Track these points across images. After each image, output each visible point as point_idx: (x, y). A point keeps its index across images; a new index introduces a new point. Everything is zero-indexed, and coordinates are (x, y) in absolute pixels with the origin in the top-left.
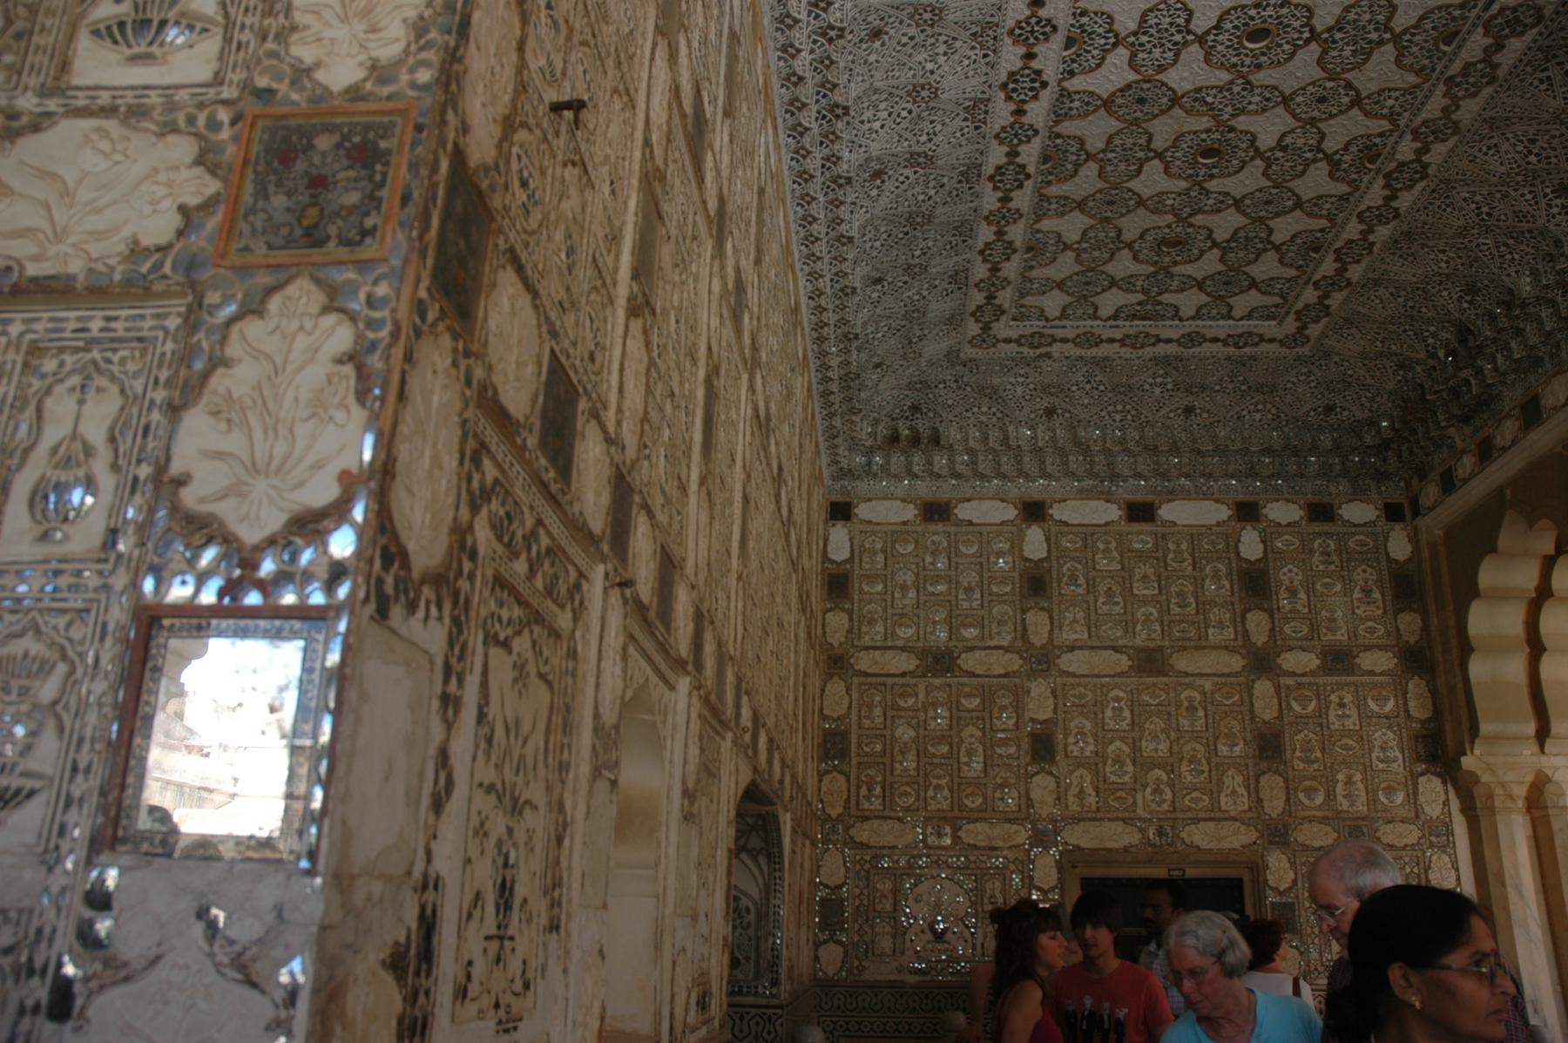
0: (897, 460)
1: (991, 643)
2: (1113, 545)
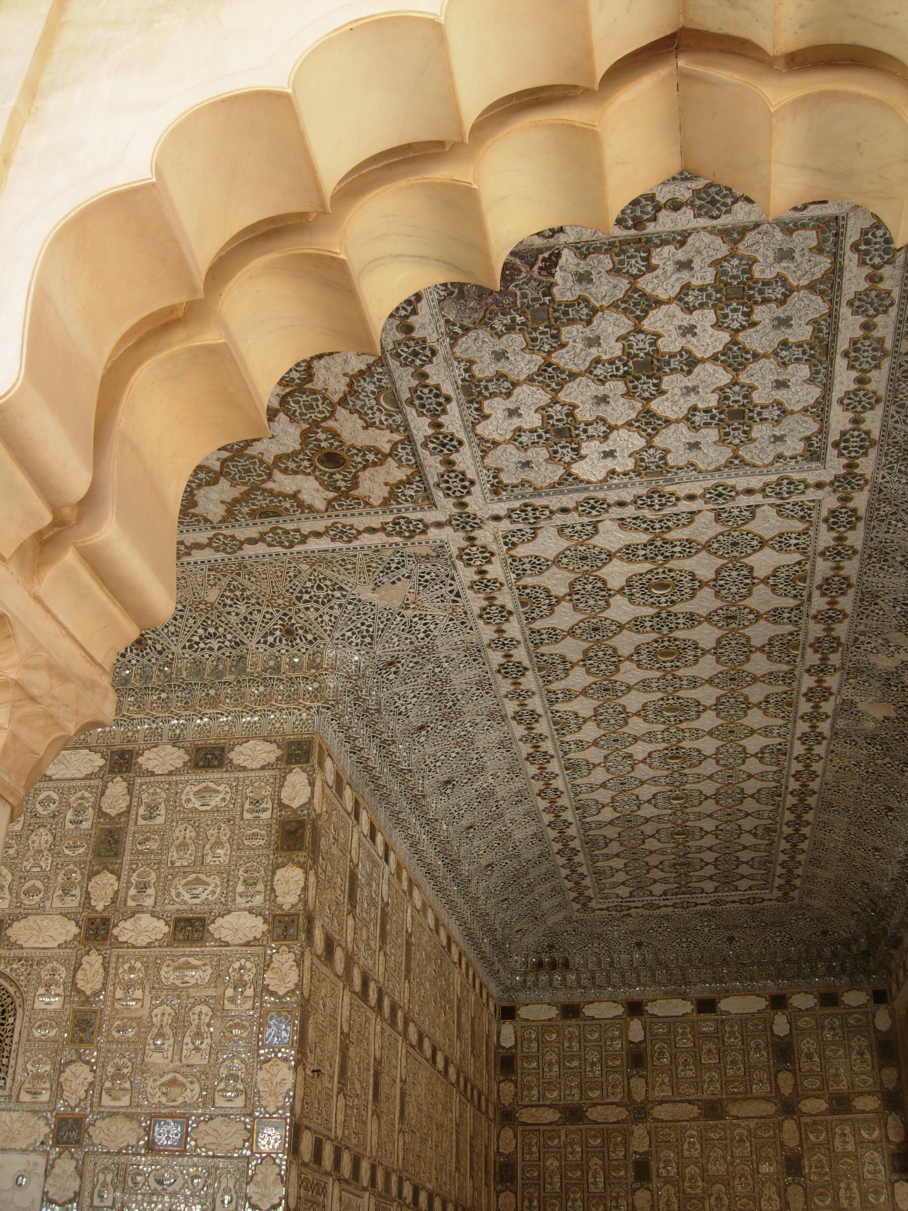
0: (544, 978)
1: (608, 1101)
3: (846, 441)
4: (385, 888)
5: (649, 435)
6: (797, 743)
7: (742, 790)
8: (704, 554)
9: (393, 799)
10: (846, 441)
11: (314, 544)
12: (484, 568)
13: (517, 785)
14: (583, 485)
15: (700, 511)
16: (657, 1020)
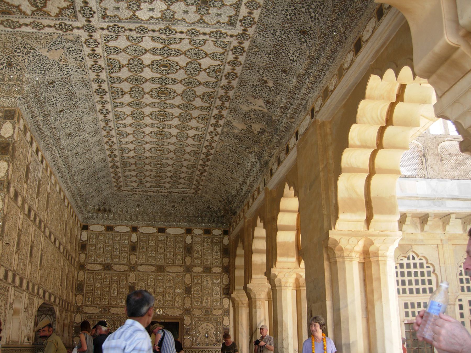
0: (100, 215)
1: (121, 263)
2: (154, 239)
3: (245, 20)
4: (41, 174)
5: (169, 4)
6: (208, 135)
7: (185, 150)
8: (183, 56)
9: (47, 139)
10: (245, 20)
11: (24, 29)
12: (95, 49)
13: (98, 138)
14: (139, 21)
15: (184, 39)
16: (142, 234)
